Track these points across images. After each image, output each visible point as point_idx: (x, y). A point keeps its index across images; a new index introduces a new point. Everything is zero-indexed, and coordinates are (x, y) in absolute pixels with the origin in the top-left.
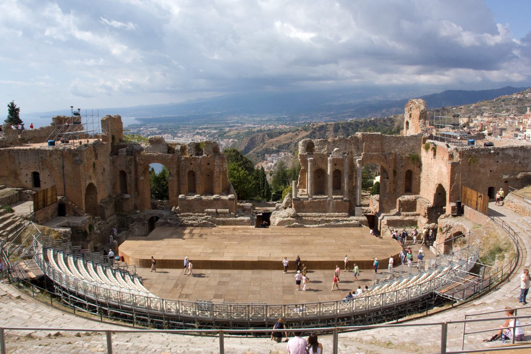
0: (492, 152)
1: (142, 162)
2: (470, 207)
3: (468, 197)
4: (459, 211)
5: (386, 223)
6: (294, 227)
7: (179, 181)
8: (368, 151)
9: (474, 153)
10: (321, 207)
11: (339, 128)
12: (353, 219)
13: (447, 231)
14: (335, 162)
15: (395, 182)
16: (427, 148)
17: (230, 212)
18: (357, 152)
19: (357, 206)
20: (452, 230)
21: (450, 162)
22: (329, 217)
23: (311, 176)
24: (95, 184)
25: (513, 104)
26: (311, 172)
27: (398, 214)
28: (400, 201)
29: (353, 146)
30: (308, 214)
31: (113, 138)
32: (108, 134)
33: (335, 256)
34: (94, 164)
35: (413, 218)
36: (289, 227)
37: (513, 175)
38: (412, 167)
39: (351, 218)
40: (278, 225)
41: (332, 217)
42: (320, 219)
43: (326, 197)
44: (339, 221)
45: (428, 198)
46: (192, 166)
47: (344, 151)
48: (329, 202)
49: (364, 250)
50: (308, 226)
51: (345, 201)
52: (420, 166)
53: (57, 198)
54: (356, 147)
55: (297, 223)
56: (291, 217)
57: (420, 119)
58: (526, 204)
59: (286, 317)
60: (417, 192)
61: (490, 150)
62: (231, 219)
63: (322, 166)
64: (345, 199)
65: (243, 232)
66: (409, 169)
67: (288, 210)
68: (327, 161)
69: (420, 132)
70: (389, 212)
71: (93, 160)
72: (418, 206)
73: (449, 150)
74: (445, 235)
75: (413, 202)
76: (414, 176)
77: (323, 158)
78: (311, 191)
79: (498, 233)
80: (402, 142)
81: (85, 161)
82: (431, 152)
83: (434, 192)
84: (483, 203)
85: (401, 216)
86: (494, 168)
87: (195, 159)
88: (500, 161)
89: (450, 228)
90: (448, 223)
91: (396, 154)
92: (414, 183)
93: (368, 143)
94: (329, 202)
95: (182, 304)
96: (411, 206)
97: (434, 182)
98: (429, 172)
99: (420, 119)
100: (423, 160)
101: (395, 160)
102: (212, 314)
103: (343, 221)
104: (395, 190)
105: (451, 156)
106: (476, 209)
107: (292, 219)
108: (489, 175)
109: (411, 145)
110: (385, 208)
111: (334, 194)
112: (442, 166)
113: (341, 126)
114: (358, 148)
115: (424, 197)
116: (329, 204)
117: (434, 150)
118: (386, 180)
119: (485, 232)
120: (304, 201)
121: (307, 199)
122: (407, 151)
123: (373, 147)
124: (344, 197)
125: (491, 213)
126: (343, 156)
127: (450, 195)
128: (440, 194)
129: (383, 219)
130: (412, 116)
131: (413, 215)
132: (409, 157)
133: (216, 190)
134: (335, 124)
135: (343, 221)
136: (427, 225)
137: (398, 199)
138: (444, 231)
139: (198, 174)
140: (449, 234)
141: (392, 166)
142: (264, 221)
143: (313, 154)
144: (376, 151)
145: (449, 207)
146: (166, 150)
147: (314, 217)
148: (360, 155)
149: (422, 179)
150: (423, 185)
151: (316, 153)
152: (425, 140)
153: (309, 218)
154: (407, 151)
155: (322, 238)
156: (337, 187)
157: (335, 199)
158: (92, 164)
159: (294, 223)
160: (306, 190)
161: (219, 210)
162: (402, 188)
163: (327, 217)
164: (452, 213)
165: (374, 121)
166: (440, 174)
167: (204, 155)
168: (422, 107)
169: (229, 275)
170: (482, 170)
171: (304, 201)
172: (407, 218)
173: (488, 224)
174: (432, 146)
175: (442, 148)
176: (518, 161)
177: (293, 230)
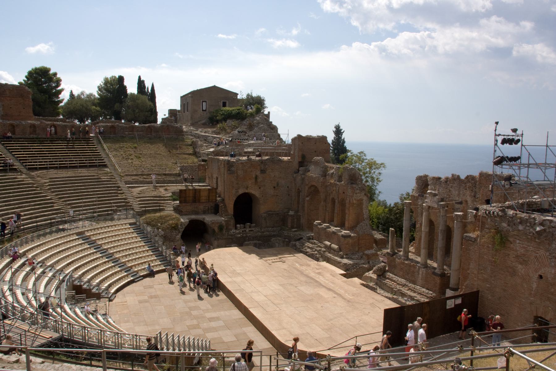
1: (307, 183)
7: (326, 206)
9: (504, 225)
17: (340, 249)
18: (473, 201)
22: (412, 290)
24: (257, 195)
29: (468, 192)
30: (395, 278)
31: (303, 157)
32: (294, 152)
34: (256, 177)
41: (415, 292)
47: (457, 199)
48: (419, 269)
50: (382, 292)
51: (434, 273)
53: (216, 200)
54: (472, 194)
55: (371, 284)
62: (336, 258)
64: (436, 271)
71: (258, 173)
81: (240, 172)
87: (336, 185)
94: (419, 269)
108: (535, 286)
114: (475, 197)
116: (418, 272)
126: (438, 205)
133: (347, 225)
147: (398, 284)
158: (254, 176)
161: (333, 245)
163: (409, 289)
167: (343, 182)
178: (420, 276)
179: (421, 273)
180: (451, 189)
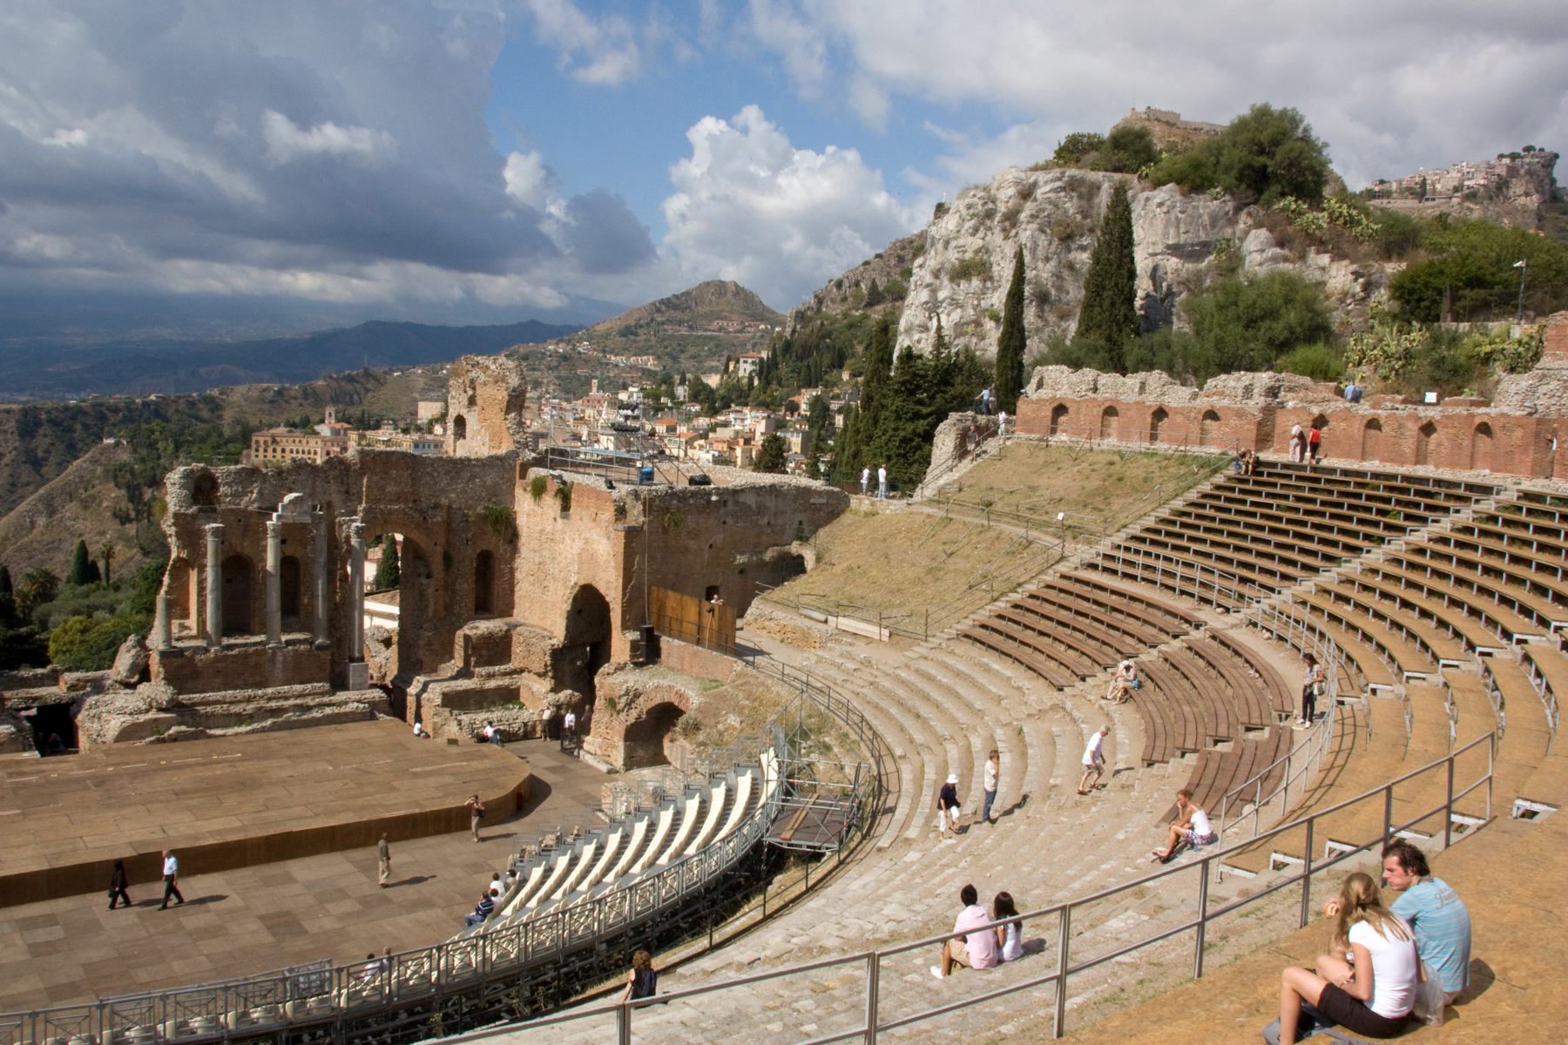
0: (714, 498)
2: (680, 638)
3: (669, 612)
4: (648, 652)
5: (438, 701)
6: (175, 739)
8: (378, 501)
10: (248, 671)
11: (38, 424)
12: (351, 699)
13: (629, 705)
14: (287, 534)
15: (449, 587)
16: (539, 489)
18: (344, 502)
19: (352, 660)
20: (641, 699)
21: (620, 526)
22: (277, 699)
23: (215, 580)
25: (550, 368)
26: (215, 566)
27: (465, 673)
28: (467, 638)
29: (333, 487)
33: (362, 808)
35: (506, 681)
36: (159, 741)
37: (757, 553)
38: (492, 542)
39: (341, 696)
40: (118, 739)
41: (286, 698)
42: (250, 707)
43: (262, 638)
44: (309, 708)
45: (547, 624)
48: (274, 653)
49: (433, 781)
51: (319, 648)
52: (512, 537)
55: (183, 728)
56: (160, 710)
57: (508, 412)
58: (808, 623)
59: (443, 981)
60: (507, 610)
61: (709, 494)
63: (246, 548)
64: (319, 641)
65: (10, 775)
66: (485, 548)
67: (143, 688)
68: (265, 531)
69: (512, 447)
70: (435, 670)
72: (517, 649)
73: (615, 494)
74: (622, 716)
75: (503, 638)
77: (249, 525)
78: (216, 626)
79: (778, 694)
82: (551, 503)
83: (567, 607)
84: (720, 628)
85: (475, 679)
86: (718, 539)
88: (730, 521)
89: (637, 695)
90: (631, 684)
91: (449, 507)
92: (498, 586)
93: (375, 478)
94: (274, 653)
95: (47, 1021)
96: (495, 650)
97: (566, 580)
98: (546, 553)
99: (508, 412)
100: (522, 521)
101: (449, 524)
102: (272, 1011)
103: (321, 706)
104: (448, 608)
105: (621, 512)
106: (699, 642)
107: (162, 715)
109: (489, 482)
110: (425, 659)
111: (287, 629)
112: (595, 536)
113: (44, 416)
114: (347, 492)
115: (530, 621)
116: (273, 660)
117: (565, 496)
118: (424, 581)
119: (741, 695)
120: (198, 657)
121: (206, 650)
122: (480, 499)
123: (389, 489)
124: (316, 637)
125: (741, 652)
126: (313, 517)
127: (624, 613)
128: (580, 612)
129: (424, 690)
130: (479, 401)
131: (505, 674)
132: (485, 517)
134: (25, 412)
135: (321, 706)
136: (552, 697)
137: (460, 633)
138: (620, 706)
140: (634, 714)
141: (442, 540)
142: (54, 730)
143: (215, 510)
144: (398, 500)
145: (621, 643)
147: (231, 703)
148: (355, 513)
149: (518, 575)
150: (524, 588)
151: (223, 506)
152: (525, 467)
153: (218, 709)
154: (480, 499)
155: (287, 762)
156: (293, 610)
157: (288, 643)
159: (174, 730)
160: (187, 623)
162: (469, 603)
163: (270, 699)
164: (632, 657)
165: (155, 403)
166: (587, 557)
168: (514, 381)
169: (50, 920)
170: (693, 545)
171: (198, 657)
172: (492, 684)
173: (739, 675)
174: (553, 486)
175: (592, 491)
176: (766, 521)
177: (179, 749)
178: (279, 665)
179: (280, 658)
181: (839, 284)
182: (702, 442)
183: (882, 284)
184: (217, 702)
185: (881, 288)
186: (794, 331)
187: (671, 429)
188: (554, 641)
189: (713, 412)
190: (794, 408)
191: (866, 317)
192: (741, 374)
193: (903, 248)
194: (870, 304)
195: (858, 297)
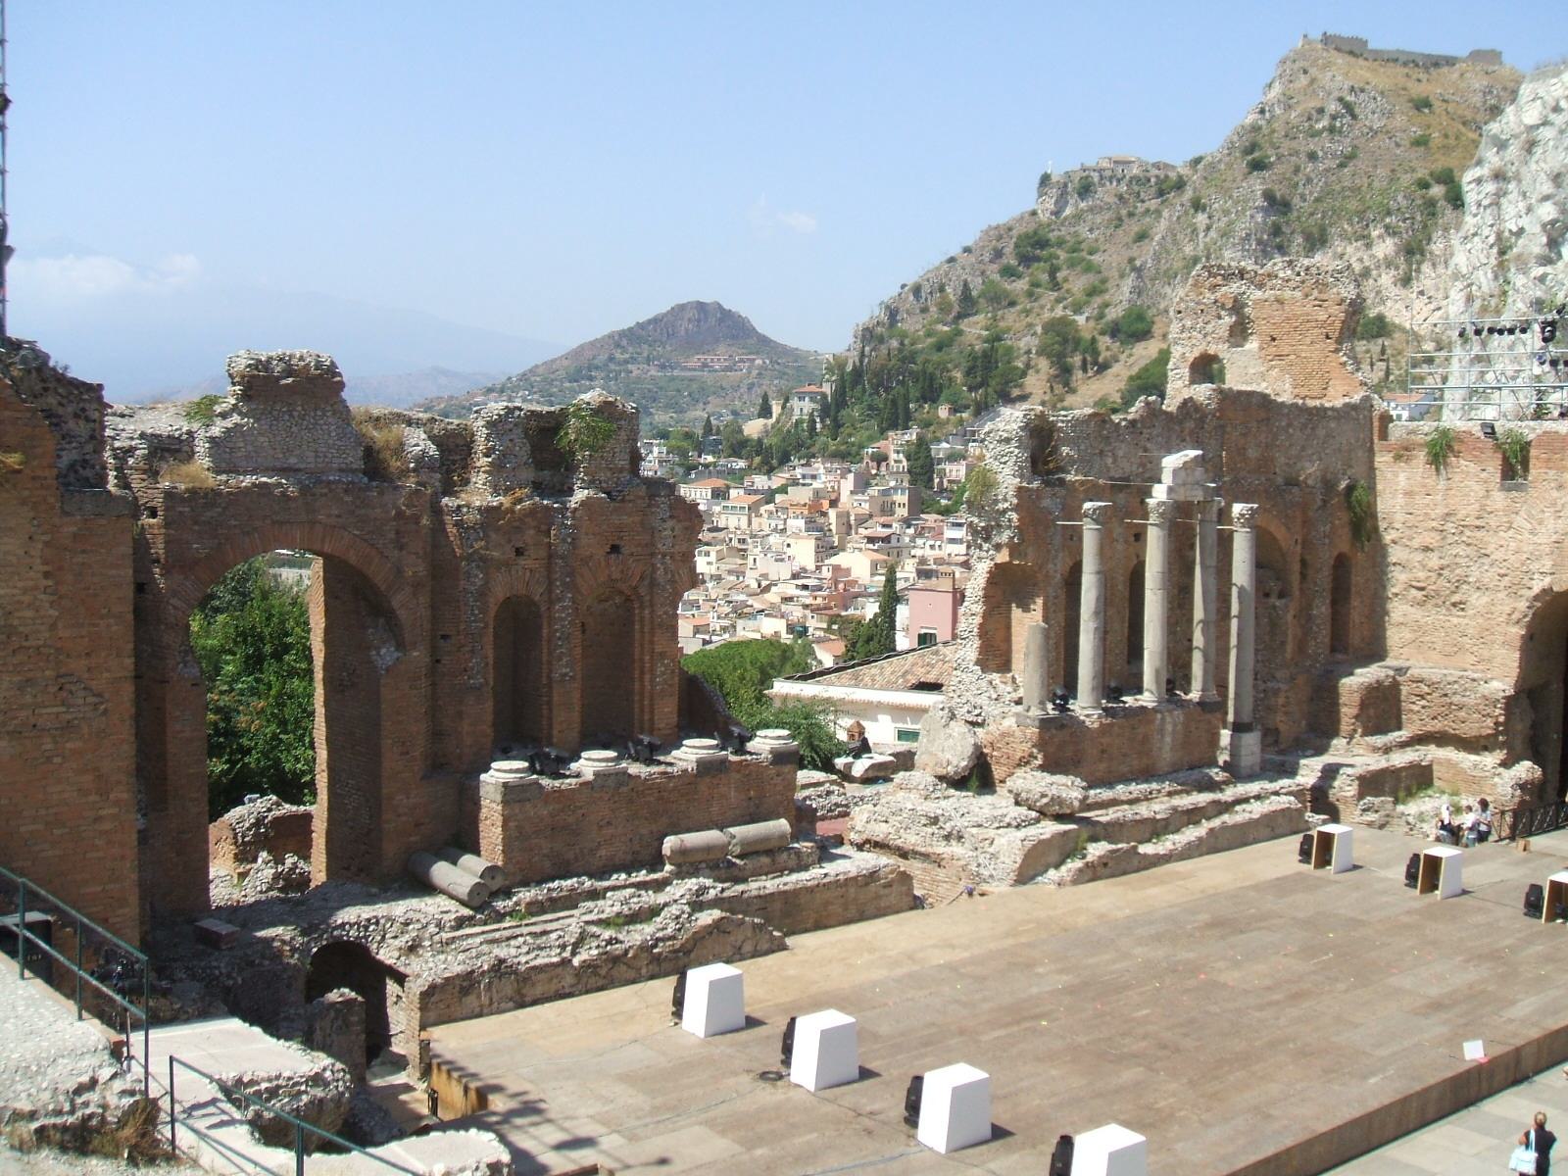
46: (522, 561)
48: (1163, 719)
76: (1357, 579)
80: (1321, 432)
94: (1163, 719)
116: (1161, 731)
139: (562, 617)
146: (355, 458)
178: (1168, 739)
179: (1169, 728)
180: (1149, 445)
181: (917, 290)
182: (771, 507)
183: (977, 285)
184: (1114, 803)
185: (974, 293)
186: (862, 355)
187: (719, 494)
188: (1496, 685)
189: (770, 471)
190: (881, 459)
191: (960, 333)
192: (797, 412)
193: (1000, 238)
194: (960, 316)
195: (945, 307)
